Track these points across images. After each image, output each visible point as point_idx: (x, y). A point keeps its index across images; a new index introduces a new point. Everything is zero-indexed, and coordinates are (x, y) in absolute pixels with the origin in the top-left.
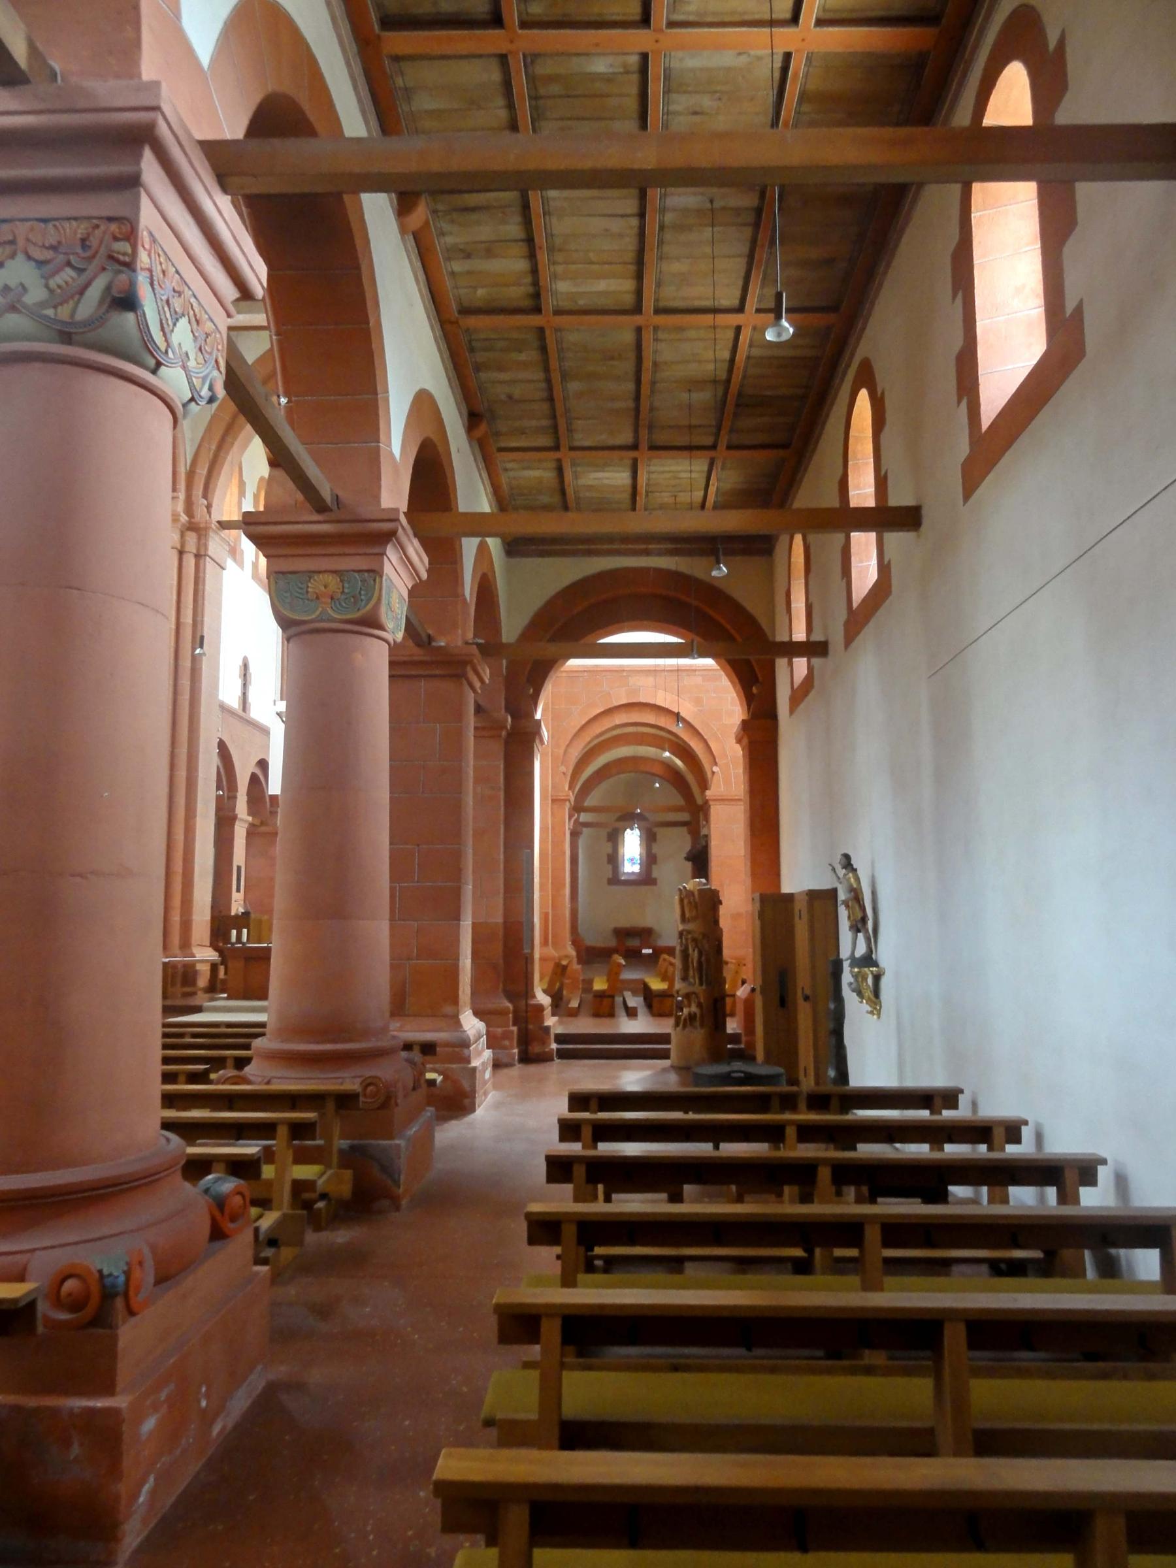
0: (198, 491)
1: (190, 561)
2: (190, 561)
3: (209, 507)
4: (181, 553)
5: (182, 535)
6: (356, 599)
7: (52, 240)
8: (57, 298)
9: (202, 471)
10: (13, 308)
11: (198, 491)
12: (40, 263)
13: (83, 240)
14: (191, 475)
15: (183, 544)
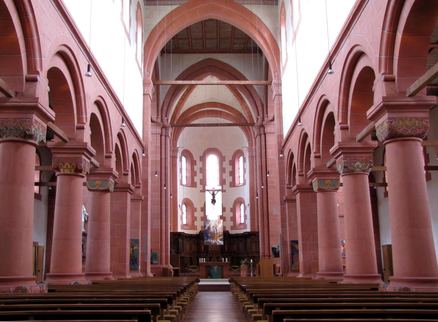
0: (164, 115)
1: (163, 137)
2: (163, 137)
3: (167, 120)
4: (161, 135)
5: (162, 130)
6: (334, 185)
7: (362, 159)
8: (363, 166)
9: (165, 108)
10: (358, 168)
11: (164, 115)
12: (361, 162)
13: (366, 160)
14: (162, 109)
15: (162, 132)
